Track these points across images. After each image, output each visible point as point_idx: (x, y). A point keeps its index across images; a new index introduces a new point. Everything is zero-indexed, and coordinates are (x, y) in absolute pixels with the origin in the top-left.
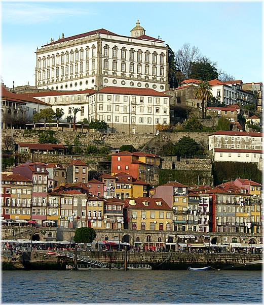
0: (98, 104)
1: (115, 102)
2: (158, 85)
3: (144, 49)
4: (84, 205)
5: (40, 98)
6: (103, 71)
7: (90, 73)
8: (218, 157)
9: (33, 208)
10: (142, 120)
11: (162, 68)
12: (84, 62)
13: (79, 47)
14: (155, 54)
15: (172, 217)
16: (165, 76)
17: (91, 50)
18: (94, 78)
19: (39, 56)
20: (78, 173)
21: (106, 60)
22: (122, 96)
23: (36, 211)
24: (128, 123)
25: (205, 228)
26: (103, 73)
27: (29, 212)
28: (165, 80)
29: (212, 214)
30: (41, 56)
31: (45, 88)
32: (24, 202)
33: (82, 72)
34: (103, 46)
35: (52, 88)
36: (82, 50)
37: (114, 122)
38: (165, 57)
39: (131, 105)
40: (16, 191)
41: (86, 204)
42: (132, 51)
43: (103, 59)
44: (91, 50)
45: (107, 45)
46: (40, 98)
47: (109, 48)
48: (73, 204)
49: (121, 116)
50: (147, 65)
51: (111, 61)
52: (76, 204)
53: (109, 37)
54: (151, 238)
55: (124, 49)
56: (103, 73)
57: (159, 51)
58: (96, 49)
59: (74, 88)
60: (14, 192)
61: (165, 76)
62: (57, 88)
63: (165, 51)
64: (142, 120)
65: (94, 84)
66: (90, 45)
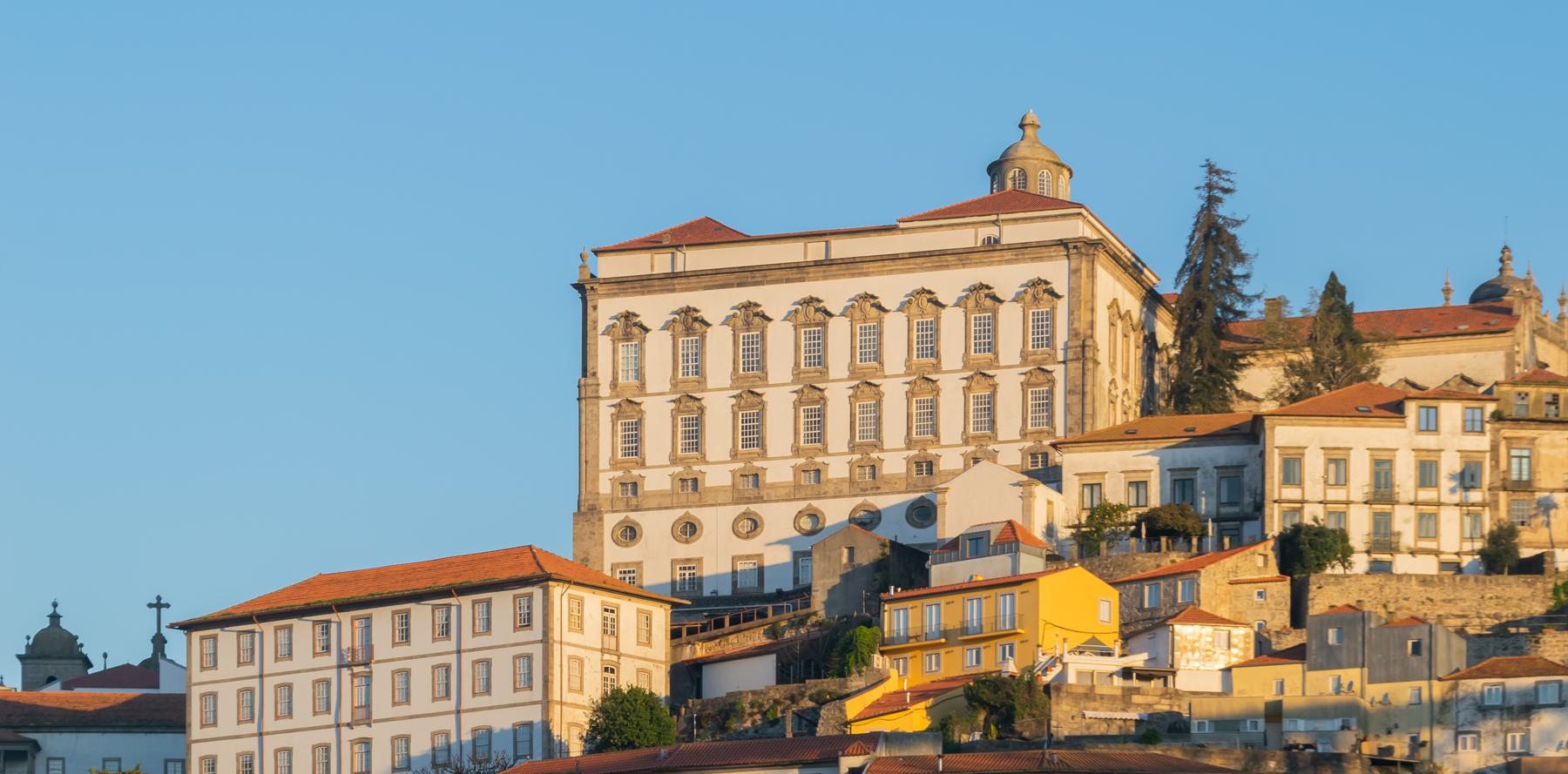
26: (605, 487)
38: (1062, 307)
56: (605, 487)
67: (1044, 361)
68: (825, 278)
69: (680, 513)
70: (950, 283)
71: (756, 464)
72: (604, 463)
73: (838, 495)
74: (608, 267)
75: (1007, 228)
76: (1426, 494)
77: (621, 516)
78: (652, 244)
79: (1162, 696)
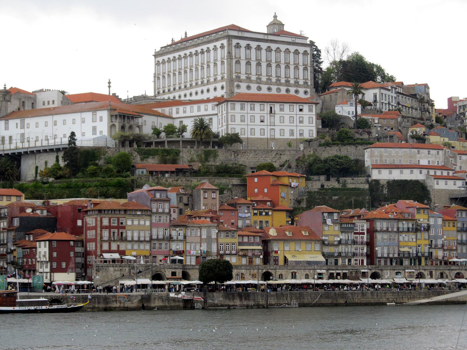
0: (229, 115)
1: (249, 111)
2: (302, 90)
3: (283, 47)
4: (214, 236)
5: (159, 110)
7: (219, 78)
8: (375, 175)
9: (153, 242)
10: (282, 131)
11: (305, 69)
12: (212, 65)
13: (205, 47)
14: (296, 52)
15: (322, 248)
16: (309, 79)
17: (219, 50)
18: (224, 83)
19: (157, 59)
20: (206, 198)
21: (238, 62)
22: (257, 106)
23: (157, 246)
24: (265, 137)
25: (363, 261)
26: (234, 77)
27: (148, 247)
28: (309, 84)
29: (371, 244)
30: (160, 59)
31: (166, 97)
32: (142, 234)
33: (210, 77)
35: (174, 97)
36: (208, 51)
37: (250, 136)
38: (309, 56)
39: (269, 115)
40: (133, 222)
41: (217, 236)
42: (269, 49)
43: (234, 61)
44: (219, 50)
45: (238, 44)
46: (159, 110)
47: (241, 47)
48: (201, 236)
50: (287, 67)
51: (243, 63)
52: (204, 236)
53: (240, 34)
54: (297, 274)
55: (259, 48)
56: (234, 77)
57: (301, 49)
58: (226, 48)
59: (200, 97)
60: (129, 223)
61: (309, 79)
62: (180, 97)
64: (282, 131)
65: (225, 90)
66: (218, 44)
72: (234, 72)
73: (274, 85)
75: (296, 39)
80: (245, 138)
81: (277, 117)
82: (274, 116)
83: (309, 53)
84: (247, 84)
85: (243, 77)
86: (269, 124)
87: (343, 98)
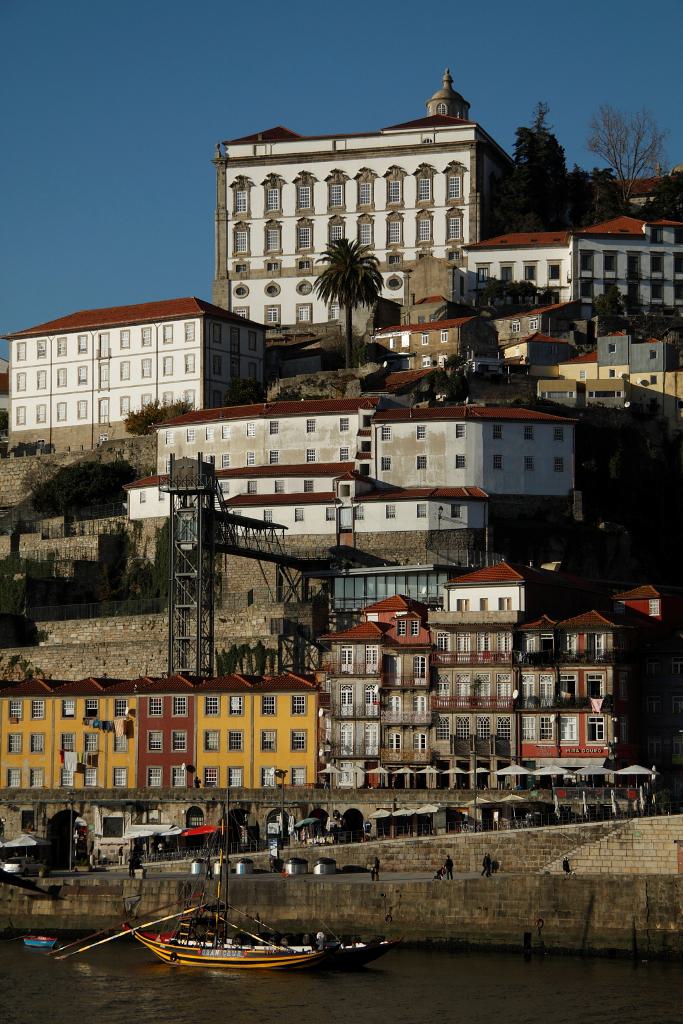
6: (230, 262)
11: (454, 212)
24: (88, 422)
26: (231, 268)
34: (230, 181)
37: (56, 424)
39: (96, 362)
43: (231, 225)
49: (72, 401)
51: (257, 228)
63: (465, 157)
67: (457, 204)
68: (343, 159)
69: (269, 281)
70: (410, 163)
71: (309, 256)
72: (230, 255)
74: (235, 151)
76: (657, 275)
77: (238, 282)
78: (251, 140)
79: (523, 379)
80: (45, 430)
81: (115, 363)
82: (108, 364)
83: (469, 169)
84: (267, 281)
85: (257, 263)
86: (96, 387)
87: (426, 285)
